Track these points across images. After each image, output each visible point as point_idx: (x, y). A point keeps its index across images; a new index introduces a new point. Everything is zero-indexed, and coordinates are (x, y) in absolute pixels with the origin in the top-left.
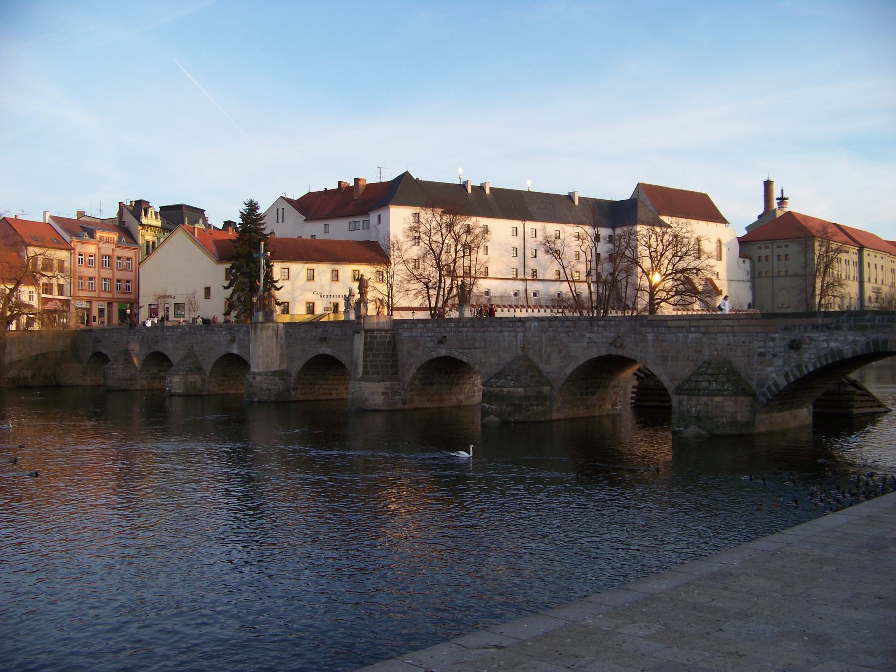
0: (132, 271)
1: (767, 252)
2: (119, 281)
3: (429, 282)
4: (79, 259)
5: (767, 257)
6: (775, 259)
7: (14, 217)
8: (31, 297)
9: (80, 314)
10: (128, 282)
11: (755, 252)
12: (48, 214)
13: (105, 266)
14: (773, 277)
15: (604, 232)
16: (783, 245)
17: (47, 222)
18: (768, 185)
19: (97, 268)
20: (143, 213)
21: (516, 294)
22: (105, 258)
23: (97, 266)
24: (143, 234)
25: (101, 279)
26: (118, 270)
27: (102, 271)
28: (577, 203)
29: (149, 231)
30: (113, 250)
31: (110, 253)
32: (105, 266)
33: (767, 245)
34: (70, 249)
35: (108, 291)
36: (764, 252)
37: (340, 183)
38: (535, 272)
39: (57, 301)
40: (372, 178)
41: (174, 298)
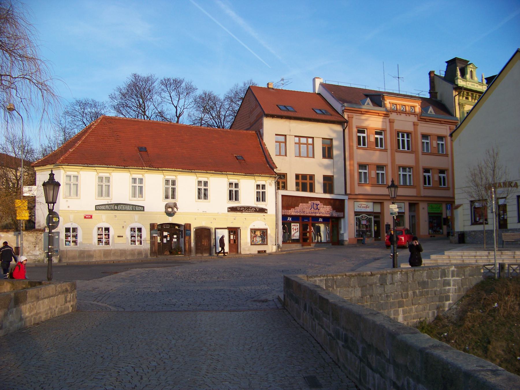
0: (447, 155)
2: (427, 170)
4: (359, 137)
7: (266, 87)
8: (261, 197)
9: (364, 222)
10: (442, 171)
12: (318, 82)
13: (403, 147)
17: (316, 92)
19: (389, 151)
20: (459, 73)
22: (403, 136)
23: (389, 147)
24: (461, 102)
25: (396, 169)
26: (423, 154)
27: (397, 155)
29: (470, 98)
30: (415, 124)
31: (409, 128)
32: (403, 147)
34: (342, 122)
35: (410, 186)
39: (318, 202)
41: (516, 185)
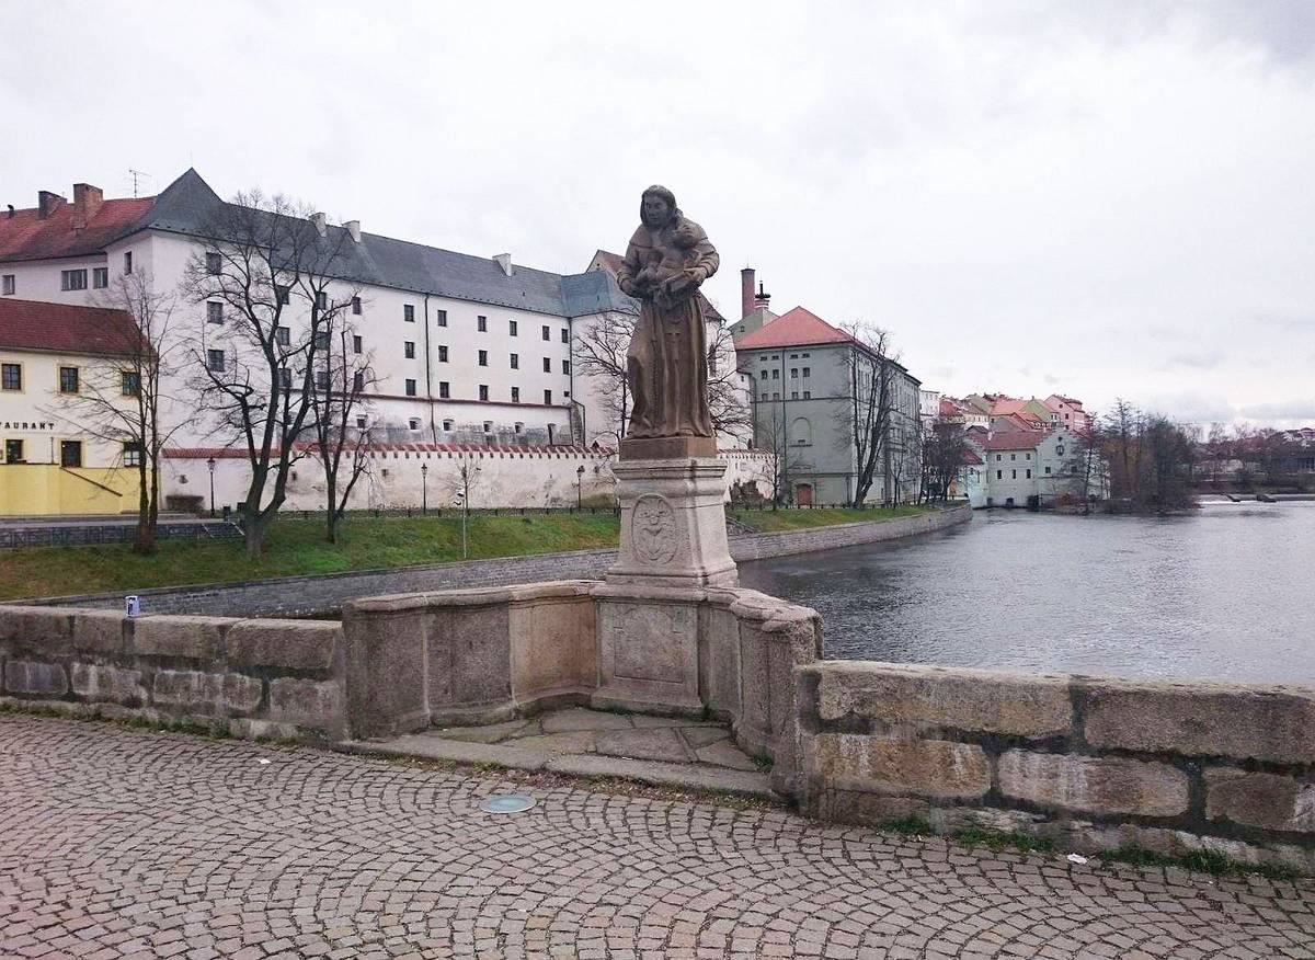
1: (777, 365)
3: (247, 394)
5: (776, 372)
6: (789, 375)
11: (758, 365)
14: (784, 401)
15: (556, 326)
16: (800, 355)
18: (748, 274)
21: (413, 425)
28: (509, 273)
33: (775, 355)
36: (770, 365)
37: (43, 195)
38: (445, 386)
40: (115, 189)
